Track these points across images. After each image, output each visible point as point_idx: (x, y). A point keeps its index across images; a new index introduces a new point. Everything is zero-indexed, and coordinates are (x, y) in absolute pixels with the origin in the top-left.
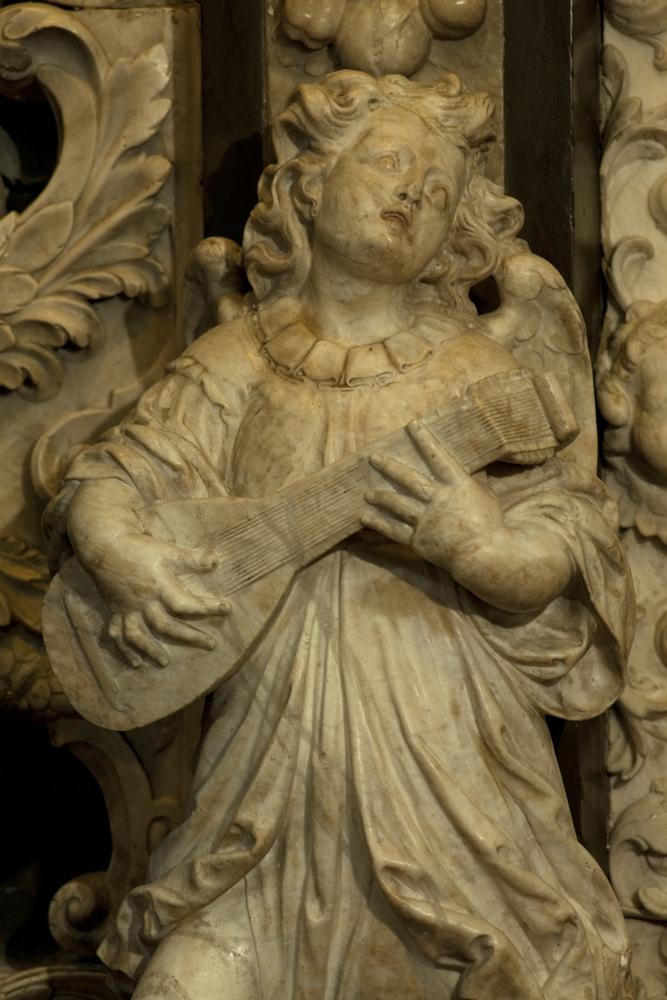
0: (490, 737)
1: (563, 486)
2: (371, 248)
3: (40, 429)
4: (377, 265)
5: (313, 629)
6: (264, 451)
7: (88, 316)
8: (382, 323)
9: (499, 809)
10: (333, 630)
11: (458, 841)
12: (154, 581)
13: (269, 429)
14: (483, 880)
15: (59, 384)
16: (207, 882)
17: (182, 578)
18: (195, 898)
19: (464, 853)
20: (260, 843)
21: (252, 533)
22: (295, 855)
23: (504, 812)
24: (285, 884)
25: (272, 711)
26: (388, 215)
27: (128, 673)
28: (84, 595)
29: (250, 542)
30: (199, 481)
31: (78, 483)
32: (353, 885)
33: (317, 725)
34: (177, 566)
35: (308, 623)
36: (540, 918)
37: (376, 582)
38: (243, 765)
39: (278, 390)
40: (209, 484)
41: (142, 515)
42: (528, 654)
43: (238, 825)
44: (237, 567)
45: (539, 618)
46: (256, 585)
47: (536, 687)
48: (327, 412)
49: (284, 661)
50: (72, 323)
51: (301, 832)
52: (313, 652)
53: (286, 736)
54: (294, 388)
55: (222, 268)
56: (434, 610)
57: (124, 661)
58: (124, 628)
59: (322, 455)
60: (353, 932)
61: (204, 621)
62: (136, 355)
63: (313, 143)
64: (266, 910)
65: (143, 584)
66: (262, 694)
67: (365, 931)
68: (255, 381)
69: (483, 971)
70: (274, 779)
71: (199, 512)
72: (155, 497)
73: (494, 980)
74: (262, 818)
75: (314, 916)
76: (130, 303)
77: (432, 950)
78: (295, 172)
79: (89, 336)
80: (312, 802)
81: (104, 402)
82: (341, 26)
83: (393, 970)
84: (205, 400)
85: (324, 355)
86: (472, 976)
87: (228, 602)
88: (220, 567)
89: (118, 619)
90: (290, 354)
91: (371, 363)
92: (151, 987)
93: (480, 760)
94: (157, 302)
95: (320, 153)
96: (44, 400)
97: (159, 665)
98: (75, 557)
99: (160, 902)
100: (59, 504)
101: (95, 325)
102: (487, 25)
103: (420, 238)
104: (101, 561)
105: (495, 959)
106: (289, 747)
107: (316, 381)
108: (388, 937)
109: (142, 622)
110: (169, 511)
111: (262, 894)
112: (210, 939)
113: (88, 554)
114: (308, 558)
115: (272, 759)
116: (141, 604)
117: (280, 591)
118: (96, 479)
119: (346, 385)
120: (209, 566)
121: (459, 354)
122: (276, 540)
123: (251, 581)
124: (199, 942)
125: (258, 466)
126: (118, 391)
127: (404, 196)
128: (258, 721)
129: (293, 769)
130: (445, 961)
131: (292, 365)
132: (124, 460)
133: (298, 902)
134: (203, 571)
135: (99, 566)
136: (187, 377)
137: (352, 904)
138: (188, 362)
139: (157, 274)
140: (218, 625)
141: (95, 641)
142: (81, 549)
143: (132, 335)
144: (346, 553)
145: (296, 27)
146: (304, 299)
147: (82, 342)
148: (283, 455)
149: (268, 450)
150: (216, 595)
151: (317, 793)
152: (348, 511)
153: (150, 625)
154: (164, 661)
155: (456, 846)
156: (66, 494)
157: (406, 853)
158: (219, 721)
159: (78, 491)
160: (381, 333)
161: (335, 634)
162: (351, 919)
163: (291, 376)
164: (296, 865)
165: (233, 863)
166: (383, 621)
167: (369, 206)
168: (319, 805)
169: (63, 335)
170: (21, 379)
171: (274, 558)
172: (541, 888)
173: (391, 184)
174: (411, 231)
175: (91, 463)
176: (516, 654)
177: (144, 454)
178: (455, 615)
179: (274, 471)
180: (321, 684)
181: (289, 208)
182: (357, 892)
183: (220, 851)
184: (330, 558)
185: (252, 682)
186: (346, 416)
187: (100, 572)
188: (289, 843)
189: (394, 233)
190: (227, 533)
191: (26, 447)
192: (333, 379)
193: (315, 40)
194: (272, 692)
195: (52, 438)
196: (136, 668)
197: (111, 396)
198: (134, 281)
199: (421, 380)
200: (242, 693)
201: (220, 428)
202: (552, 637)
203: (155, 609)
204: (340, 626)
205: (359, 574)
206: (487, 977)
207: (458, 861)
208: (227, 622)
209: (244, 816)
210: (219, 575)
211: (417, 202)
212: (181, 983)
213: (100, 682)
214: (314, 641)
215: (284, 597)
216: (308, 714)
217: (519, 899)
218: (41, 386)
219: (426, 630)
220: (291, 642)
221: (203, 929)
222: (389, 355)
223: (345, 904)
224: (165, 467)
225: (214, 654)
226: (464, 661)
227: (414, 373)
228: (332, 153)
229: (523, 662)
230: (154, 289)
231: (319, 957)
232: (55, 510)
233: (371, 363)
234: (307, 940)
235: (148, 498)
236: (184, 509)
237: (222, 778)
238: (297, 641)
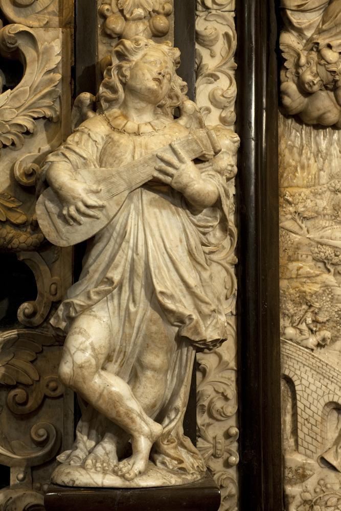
0: (192, 250)
1: (213, 169)
2: (150, 90)
3: (16, 159)
4: (150, 96)
5: (133, 213)
6: (113, 155)
7: (33, 123)
8: (148, 117)
9: (193, 274)
10: (141, 213)
11: (182, 284)
12: (80, 195)
13: (114, 148)
14: (188, 297)
15: (23, 145)
16: (95, 297)
17: (88, 195)
18: (90, 303)
19: (183, 288)
20: (115, 284)
21: (114, 180)
22: (125, 289)
23: (194, 275)
24: (121, 298)
25: (118, 240)
26: (155, 79)
27: (68, 227)
28: (51, 201)
29: (113, 182)
30: (92, 164)
31: (50, 163)
32: (145, 298)
33: (135, 245)
34: (88, 191)
35: (131, 211)
36: (205, 309)
37: (154, 198)
38: (107, 259)
39: (116, 136)
40: (94, 165)
41: (74, 173)
42: (202, 224)
43: (107, 278)
44: (108, 191)
45: (202, 213)
46: (115, 197)
47: (202, 235)
48: (134, 143)
49: (123, 224)
50: (28, 124)
51: (128, 281)
52: (133, 221)
53: (125, 249)
54: (121, 135)
55: (88, 102)
56: (173, 207)
57: (67, 222)
58: (68, 211)
59: (133, 157)
60: (145, 314)
61: (97, 209)
62: (48, 137)
63: (126, 58)
64: (114, 307)
65: (77, 196)
66: (115, 235)
67: (149, 314)
68: (107, 133)
69: (190, 326)
70: (120, 262)
71: (95, 173)
72: (78, 168)
73: (193, 329)
74: (116, 276)
75: (132, 308)
76: (45, 121)
77: (172, 320)
78: (120, 68)
79: (33, 130)
80: (133, 270)
81: (37, 151)
82: (124, 30)
83: (158, 327)
84: (91, 140)
85: (131, 126)
86: (185, 328)
87: (105, 203)
88: (102, 191)
89: (66, 208)
90: (119, 125)
91: (148, 129)
92: (75, 332)
93: (188, 258)
94: (55, 120)
95: (129, 61)
96: (17, 150)
97: (80, 224)
98: (49, 188)
99: (77, 304)
100: (43, 170)
101: (35, 126)
102: (169, 33)
103: (164, 88)
104: (61, 188)
105: (194, 322)
106: (126, 252)
107: (129, 133)
108: (156, 316)
109: (75, 210)
110: (84, 172)
111: (113, 301)
112: (95, 316)
113: (56, 186)
114: (134, 188)
115: (120, 256)
116: (76, 203)
117: (123, 200)
118: (58, 161)
119: (139, 135)
120: (99, 190)
121: (174, 127)
122: (122, 182)
123: (113, 196)
124: (92, 317)
125: (111, 160)
126: (42, 148)
127: (160, 74)
128: (113, 243)
129: (126, 259)
130: (176, 323)
131: (120, 128)
132: (68, 155)
133: (125, 304)
134: (97, 192)
135: (60, 190)
136: (83, 132)
137: (144, 305)
138: (83, 128)
139: (56, 111)
140: (101, 211)
141: (56, 216)
142: (54, 184)
143: (46, 130)
144: (142, 189)
145: (109, 29)
146: (122, 109)
147: (31, 132)
148: (120, 157)
149: (114, 155)
150: (101, 200)
151: (135, 267)
152: (148, 172)
153: (78, 210)
154: (82, 222)
155: (181, 286)
156: (46, 167)
157: (166, 287)
158: (98, 244)
159: (51, 166)
160: (148, 120)
161: (141, 215)
162: (144, 310)
163: (120, 132)
164: (125, 292)
165: (105, 291)
166: (157, 210)
167: (148, 76)
168: (136, 271)
169: (25, 128)
170: (11, 143)
171: (122, 188)
172: (207, 300)
173: (155, 70)
174: (161, 85)
175: (54, 157)
176: (198, 224)
177: (74, 154)
178: (180, 210)
179: (117, 162)
180: (136, 231)
181: (117, 79)
182: (146, 301)
183: (99, 287)
184: (137, 190)
185: (111, 231)
186: (141, 144)
187: (61, 192)
188: (124, 284)
189: (157, 85)
190: (105, 179)
191: (11, 165)
192: (135, 133)
193: (116, 34)
194: (118, 234)
195: (21, 161)
196: (71, 225)
197: (40, 149)
198: (49, 113)
199: (163, 135)
200: (107, 235)
201: (96, 149)
202: (206, 219)
203: (80, 205)
204: (143, 212)
205: (148, 196)
206: (191, 329)
207: (181, 291)
208: (104, 210)
209: (109, 275)
210: (102, 193)
211: (164, 76)
212: (87, 330)
213: (57, 231)
214: (133, 217)
215: (124, 202)
216: (132, 241)
217: (200, 303)
218: (17, 145)
219: (171, 214)
220: (125, 217)
221: (92, 313)
222: (152, 127)
223: (142, 305)
224: (81, 158)
225: (99, 221)
226: (183, 225)
227: (161, 132)
228: (133, 61)
229: (200, 226)
230: (54, 116)
231: (133, 322)
232: (42, 173)
233: (147, 129)
234: (129, 317)
235: (76, 168)
236: (89, 172)
237: (99, 263)
238: (128, 217)
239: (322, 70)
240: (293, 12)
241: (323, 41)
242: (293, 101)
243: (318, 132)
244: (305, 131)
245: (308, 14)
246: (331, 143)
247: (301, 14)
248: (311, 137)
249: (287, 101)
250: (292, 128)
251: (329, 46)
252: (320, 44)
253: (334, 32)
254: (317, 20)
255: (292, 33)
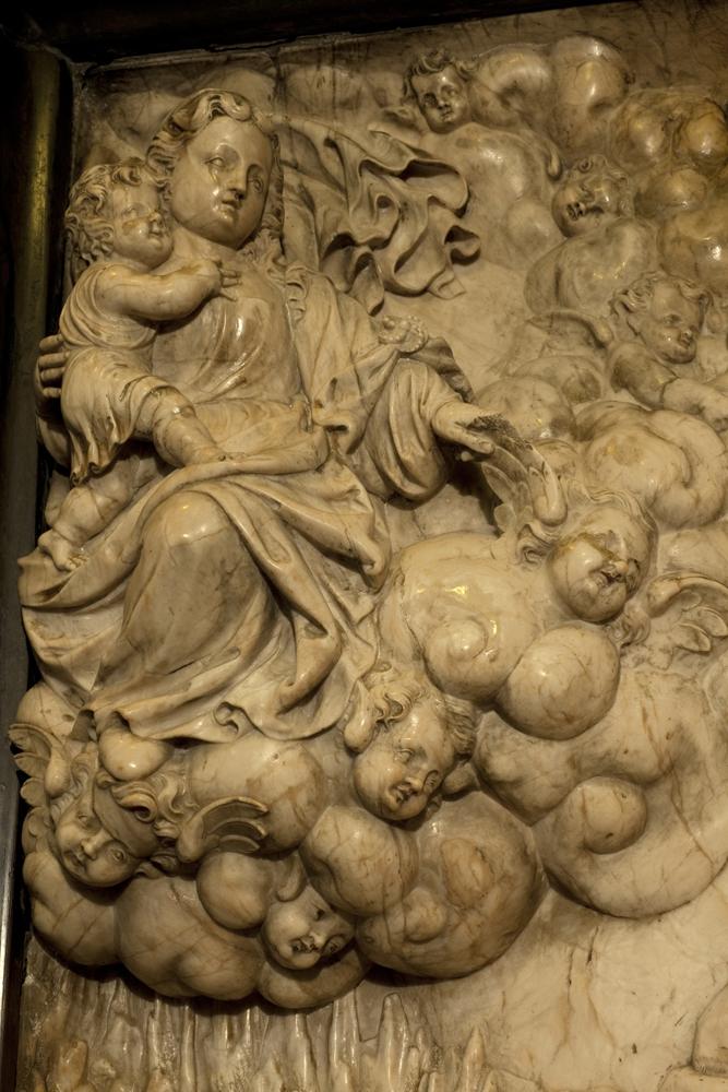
239: (106, 805)
240: (41, 616)
241: (102, 708)
242: (59, 918)
243: (212, 1026)
244: (162, 1022)
245: (87, 618)
246: (255, 1064)
247: (66, 622)
248: (180, 1041)
249: (43, 917)
250: (113, 1015)
251: (124, 723)
252: (97, 715)
253: (138, 670)
254: (113, 633)
255: (50, 687)
